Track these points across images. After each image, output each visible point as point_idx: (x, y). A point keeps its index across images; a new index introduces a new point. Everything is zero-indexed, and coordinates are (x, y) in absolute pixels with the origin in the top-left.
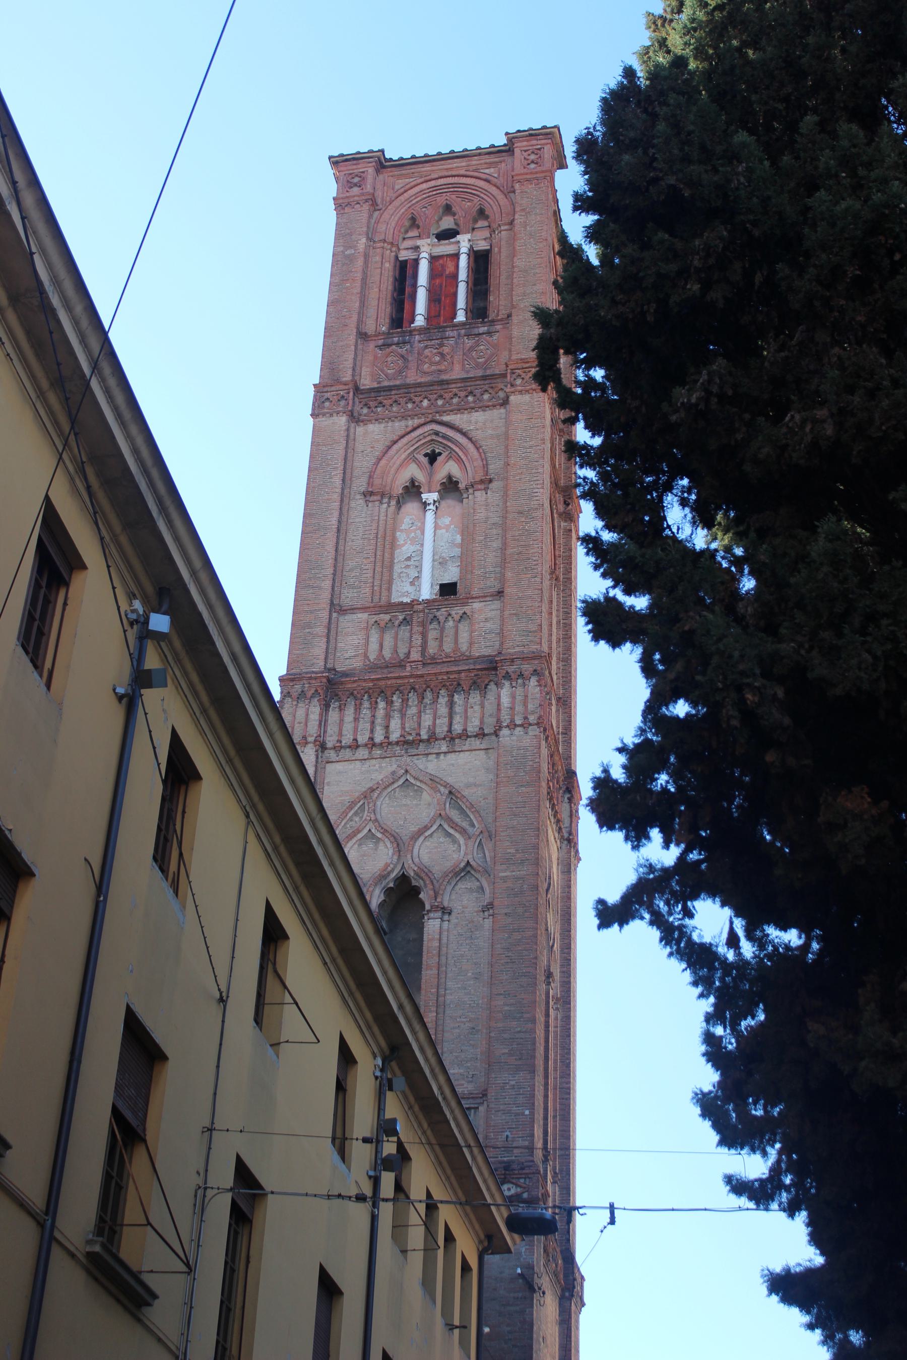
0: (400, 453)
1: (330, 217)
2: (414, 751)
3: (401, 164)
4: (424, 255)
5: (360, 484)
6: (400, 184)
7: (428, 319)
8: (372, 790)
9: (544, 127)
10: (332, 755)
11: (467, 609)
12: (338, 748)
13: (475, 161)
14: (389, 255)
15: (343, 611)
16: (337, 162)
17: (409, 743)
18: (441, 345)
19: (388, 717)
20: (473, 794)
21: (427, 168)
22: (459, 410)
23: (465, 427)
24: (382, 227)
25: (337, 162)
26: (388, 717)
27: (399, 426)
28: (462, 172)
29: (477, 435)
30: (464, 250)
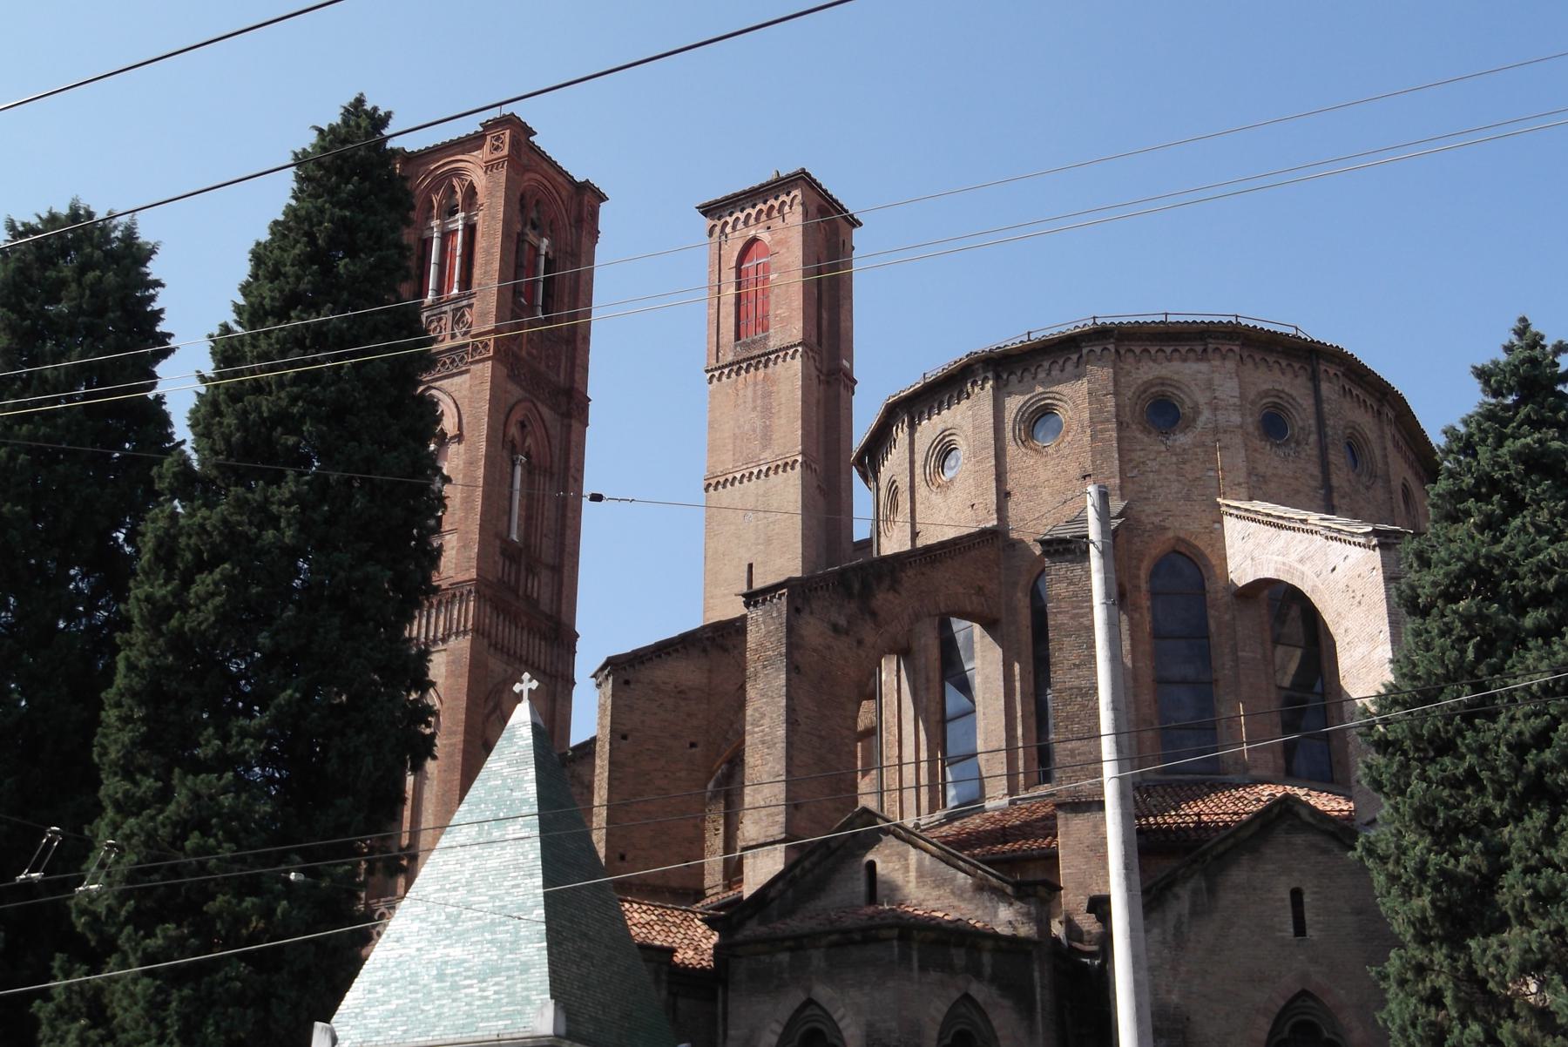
18: (441, 319)
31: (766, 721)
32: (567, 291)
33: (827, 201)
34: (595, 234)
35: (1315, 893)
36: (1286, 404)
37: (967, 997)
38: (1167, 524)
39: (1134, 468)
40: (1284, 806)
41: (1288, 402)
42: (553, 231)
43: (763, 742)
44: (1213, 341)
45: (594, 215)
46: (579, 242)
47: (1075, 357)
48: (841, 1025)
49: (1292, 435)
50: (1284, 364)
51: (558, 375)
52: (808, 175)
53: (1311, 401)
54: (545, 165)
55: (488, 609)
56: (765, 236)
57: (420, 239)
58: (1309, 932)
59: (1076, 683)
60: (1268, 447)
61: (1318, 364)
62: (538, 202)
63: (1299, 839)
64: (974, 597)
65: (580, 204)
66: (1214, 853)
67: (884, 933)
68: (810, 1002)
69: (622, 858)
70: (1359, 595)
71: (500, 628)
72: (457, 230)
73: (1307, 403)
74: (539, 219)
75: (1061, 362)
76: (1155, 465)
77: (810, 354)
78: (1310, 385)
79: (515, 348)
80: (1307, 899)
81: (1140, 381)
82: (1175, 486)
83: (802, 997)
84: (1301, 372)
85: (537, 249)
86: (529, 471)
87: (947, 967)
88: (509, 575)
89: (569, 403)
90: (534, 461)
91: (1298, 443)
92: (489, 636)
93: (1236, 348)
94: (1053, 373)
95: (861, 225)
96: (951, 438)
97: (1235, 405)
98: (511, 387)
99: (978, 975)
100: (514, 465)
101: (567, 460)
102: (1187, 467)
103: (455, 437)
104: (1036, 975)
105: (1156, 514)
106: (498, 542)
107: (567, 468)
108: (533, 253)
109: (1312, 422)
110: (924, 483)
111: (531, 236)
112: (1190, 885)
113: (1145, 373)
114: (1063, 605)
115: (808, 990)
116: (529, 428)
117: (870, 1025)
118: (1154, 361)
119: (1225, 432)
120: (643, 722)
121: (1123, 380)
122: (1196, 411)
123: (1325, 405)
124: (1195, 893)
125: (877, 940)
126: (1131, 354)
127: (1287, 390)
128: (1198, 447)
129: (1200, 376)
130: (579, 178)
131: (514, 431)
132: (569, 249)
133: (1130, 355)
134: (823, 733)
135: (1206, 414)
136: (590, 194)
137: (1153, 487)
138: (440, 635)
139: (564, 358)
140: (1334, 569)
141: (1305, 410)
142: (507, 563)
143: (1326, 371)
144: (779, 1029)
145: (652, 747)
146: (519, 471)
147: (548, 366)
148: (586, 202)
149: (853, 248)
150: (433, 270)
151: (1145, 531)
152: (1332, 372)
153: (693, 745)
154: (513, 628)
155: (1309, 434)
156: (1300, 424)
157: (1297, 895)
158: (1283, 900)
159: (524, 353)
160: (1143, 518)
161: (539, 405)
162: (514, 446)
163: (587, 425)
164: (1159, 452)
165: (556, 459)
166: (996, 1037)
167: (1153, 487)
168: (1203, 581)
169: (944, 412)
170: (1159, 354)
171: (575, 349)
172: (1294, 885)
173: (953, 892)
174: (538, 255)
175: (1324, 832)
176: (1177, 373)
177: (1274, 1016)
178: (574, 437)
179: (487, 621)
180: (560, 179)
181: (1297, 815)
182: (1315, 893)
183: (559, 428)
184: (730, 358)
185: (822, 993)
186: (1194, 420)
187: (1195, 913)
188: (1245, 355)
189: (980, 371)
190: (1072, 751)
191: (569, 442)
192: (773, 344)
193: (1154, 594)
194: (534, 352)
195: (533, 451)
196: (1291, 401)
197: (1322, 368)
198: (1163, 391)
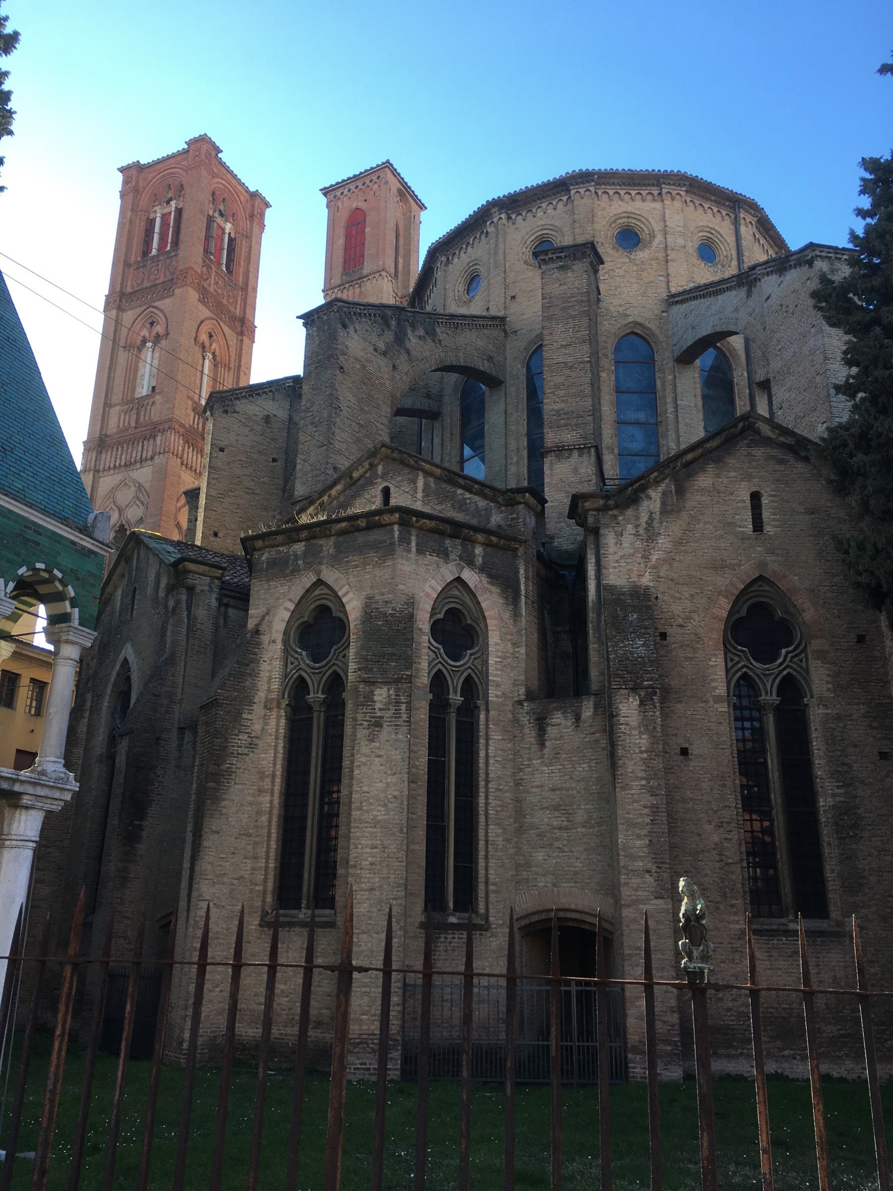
0: (138, 325)
1: (119, 202)
2: (128, 469)
3: (149, 166)
4: (158, 215)
5: (122, 343)
6: (150, 176)
7: (158, 250)
8: (113, 488)
9: (200, 136)
10: (101, 474)
11: (154, 399)
12: (104, 470)
13: (178, 158)
14: (144, 218)
15: (111, 406)
16: (122, 170)
17: (128, 465)
18: (158, 265)
19: (122, 454)
20: (147, 486)
21: (160, 165)
22: (160, 300)
23: (162, 307)
24: (141, 203)
25: (122, 170)
26: (122, 454)
27: (139, 310)
28: (173, 166)
29: (166, 311)
30: (173, 209)
31: (315, 408)
32: (243, 258)
33: (404, 187)
34: (262, 227)
35: (773, 496)
36: (715, 239)
37: (459, 580)
38: (628, 312)
39: (606, 273)
40: (747, 423)
41: (716, 237)
42: (234, 217)
43: (312, 423)
44: (666, 186)
45: (262, 215)
46: (251, 229)
47: (565, 198)
48: (344, 600)
49: (719, 261)
50: (715, 210)
51: (235, 308)
52: (392, 165)
53: (733, 238)
54: (229, 176)
55: (181, 442)
56: (362, 205)
57: (148, 218)
58: (769, 529)
59: (561, 360)
60: (703, 265)
61: (739, 212)
62: (224, 199)
63: (759, 452)
64: (485, 361)
65: (253, 206)
66: (684, 460)
67: (386, 518)
68: (320, 583)
69: (216, 534)
70: (792, 307)
71: (190, 455)
72: (171, 212)
73: (731, 239)
74: (225, 210)
75: (554, 203)
76: (621, 272)
77: (390, 278)
78: (733, 227)
79: (206, 285)
80: (765, 501)
81: (612, 214)
82: (635, 287)
83: (314, 579)
84: (727, 217)
85: (223, 230)
86: (215, 364)
87: (444, 554)
88: (198, 424)
89: (242, 326)
90: (218, 359)
91: (723, 266)
92: (181, 458)
93: (683, 193)
94: (548, 211)
95: (426, 208)
96: (475, 267)
97: (680, 232)
98: (201, 307)
99: (470, 562)
100: (204, 358)
101: (240, 361)
102: (645, 274)
103: (164, 335)
104: (522, 571)
105: (620, 305)
106: (190, 403)
107: (239, 366)
108: (220, 233)
109: (734, 253)
110: (453, 302)
111: (219, 220)
112: (663, 486)
113: (616, 209)
114: (554, 300)
115: (319, 573)
116: (215, 337)
117: (369, 598)
118: (622, 200)
119: (673, 249)
120: (237, 440)
121: (599, 213)
122: (652, 236)
123: (743, 241)
124: (664, 494)
125: (380, 525)
126: (606, 196)
127: (716, 228)
128: (652, 260)
129: (655, 212)
130: (252, 189)
131: (204, 337)
132: (245, 234)
133: (605, 196)
134: (361, 422)
135: (659, 238)
136: (259, 200)
137: (619, 287)
138: (149, 456)
139: (239, 299)
140: (768, 298)
141: (728, 244)
142: (197, 417)
143: (744, 218)
144: (292, 607)
145: (243, 459)
146: (207, 362)
147: (229, 302)
148: (256, 205)
149: (420, 222)
150: (156, 237)
151: (612, 317)
152: (748, 220)
153: (274, 460)
154: (199, 456)
155: (731, 260)
156: (725, 254)
157: (755, 497)
158: (744, 501)
159: (211, 290)
160: (611, 307)
161: (222, 324)
162: (203, 347)
163: (254, 342)
164: (624, 263)
165: (232, 359)
166: (484, 618)
167: (619, 287)
168: (653, 354)
169: (470, 249)
170: (627, 195)
171: (247, 294)
172: (753, 489)
173: (453, 506)
174: (224, 233)
175: (783, 446)
176: (639, 209)
177: (734, 598)
178: (244, 347)
179: (180, 448)
180: (240, 188)
181: (758, 432)
182: (773, 496)
183: (235, 342)
184: (339, 282)
185: (330, 576)
186: (650, 242)
187: (664, 512)
188: (688, 199)
189: (497, 213)
190: (558, 411)
191: (241, 350)
192: (365, 272)
193: (617, 362)
194: (219, 291)
195: (217, 353)
196: (719, 236)
197: (742, 216)
198: (628, 222)
